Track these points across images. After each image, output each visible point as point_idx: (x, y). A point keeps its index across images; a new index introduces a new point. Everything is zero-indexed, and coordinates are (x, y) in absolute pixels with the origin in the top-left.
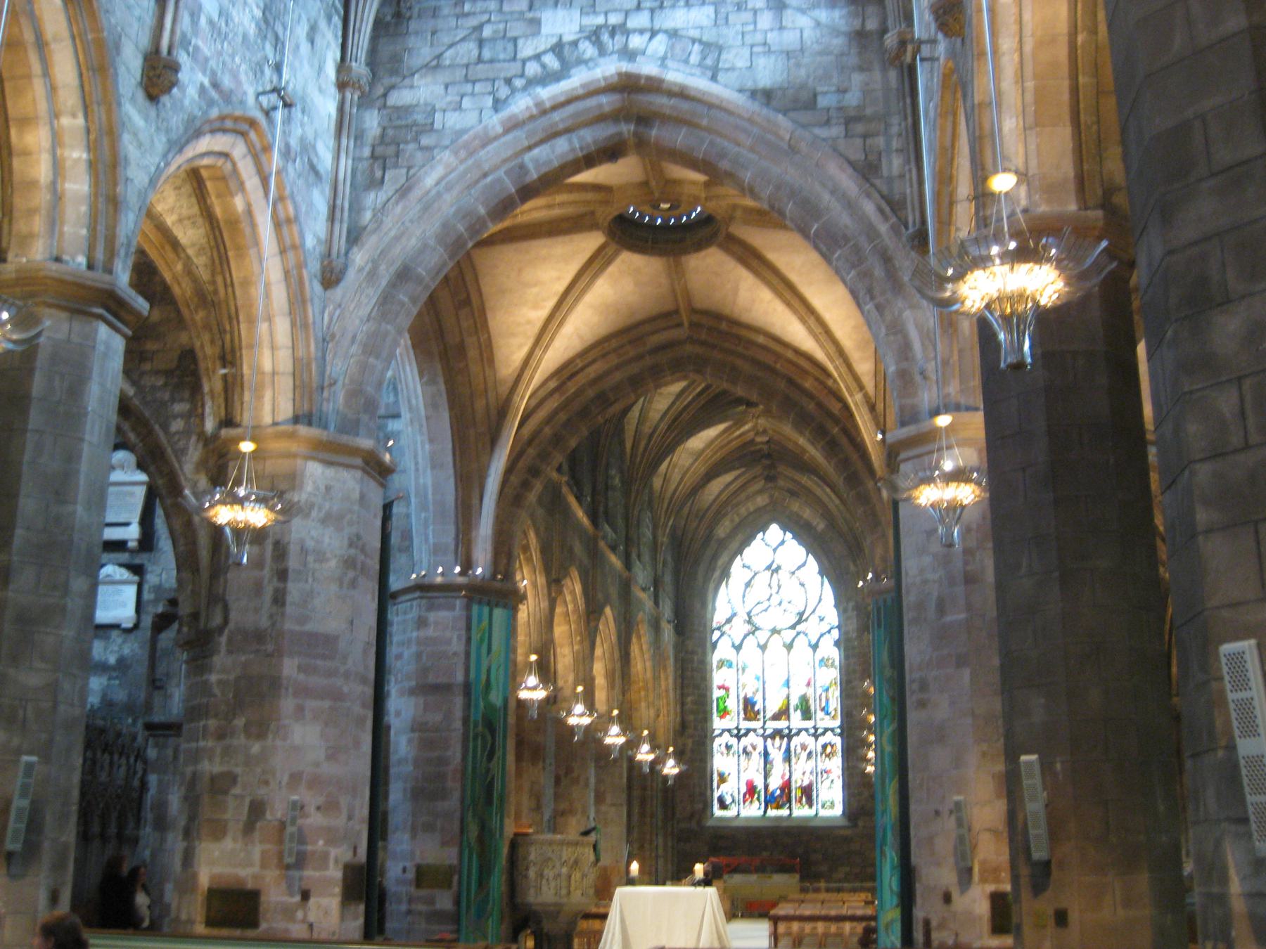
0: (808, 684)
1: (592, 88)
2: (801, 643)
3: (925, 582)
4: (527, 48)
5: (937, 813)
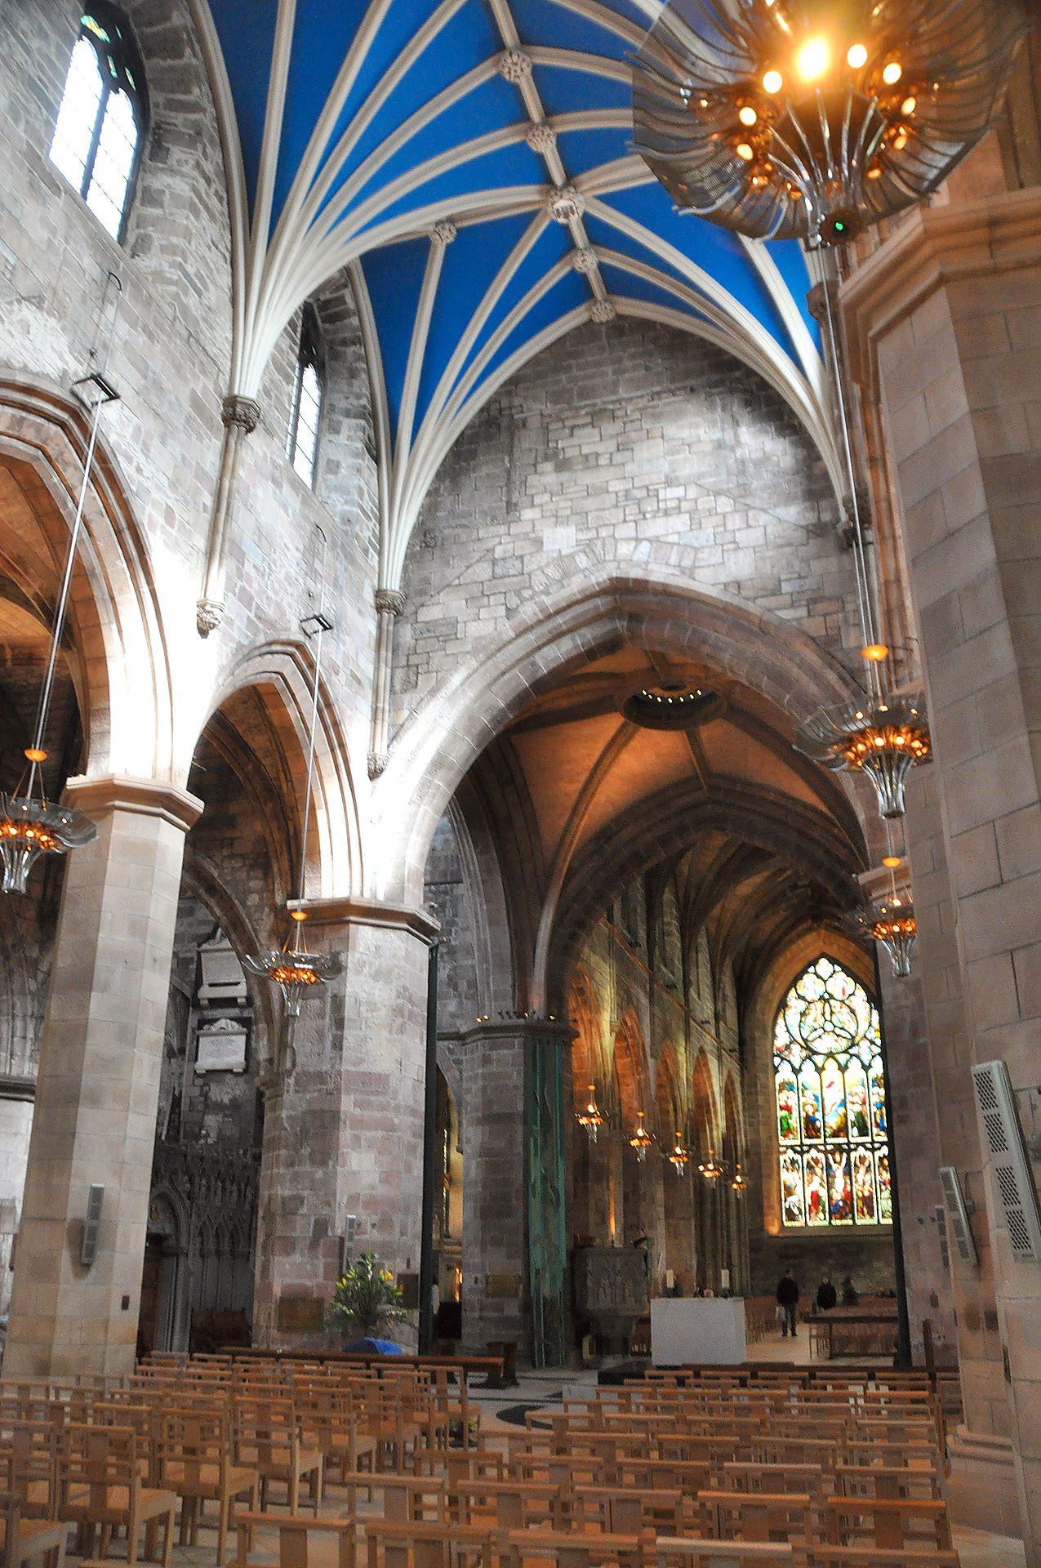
1: (588, 593)
2: (855, 1064)
3: (899, 1008)
4: (531, 565)
5: (921, 1221)
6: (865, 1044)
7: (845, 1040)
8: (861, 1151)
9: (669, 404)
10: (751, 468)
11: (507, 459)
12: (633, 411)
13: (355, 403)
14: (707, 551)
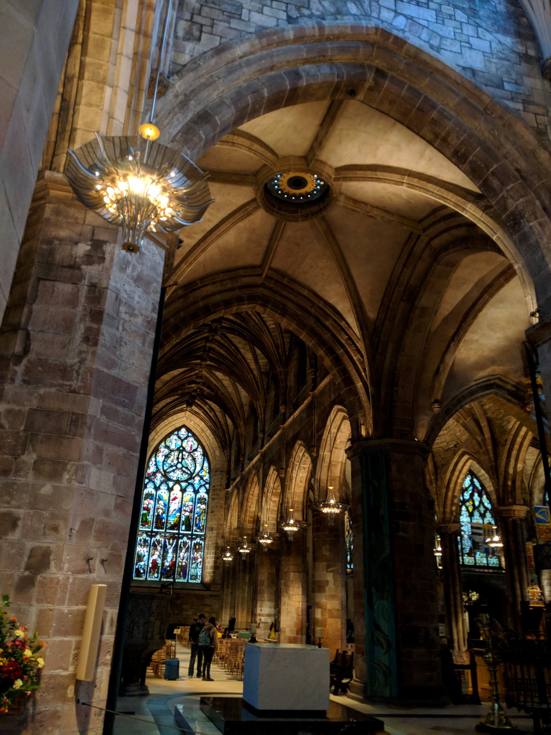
0: (191, 512)
2: (190, 489)
6: (197, 479)
7: (187, 476)
8: (185, 539)
14: (449, 41)
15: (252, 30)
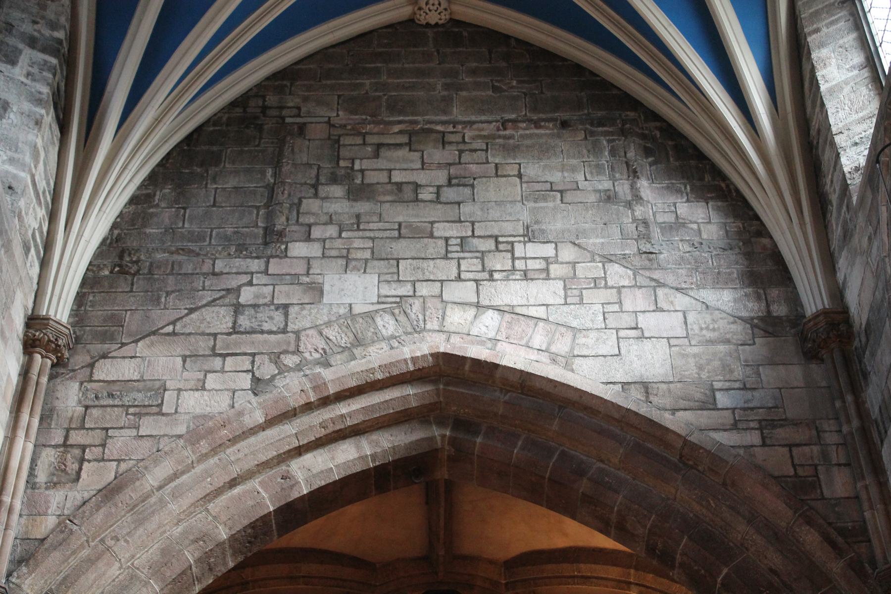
1: (395, 372)
4: (300, 319)
9: (531, 136)
10: (656, 232)
11: (269, 172)
12: (474, 138)
13: (47, 32)
14: (593, 335)
15: (181, 429)
